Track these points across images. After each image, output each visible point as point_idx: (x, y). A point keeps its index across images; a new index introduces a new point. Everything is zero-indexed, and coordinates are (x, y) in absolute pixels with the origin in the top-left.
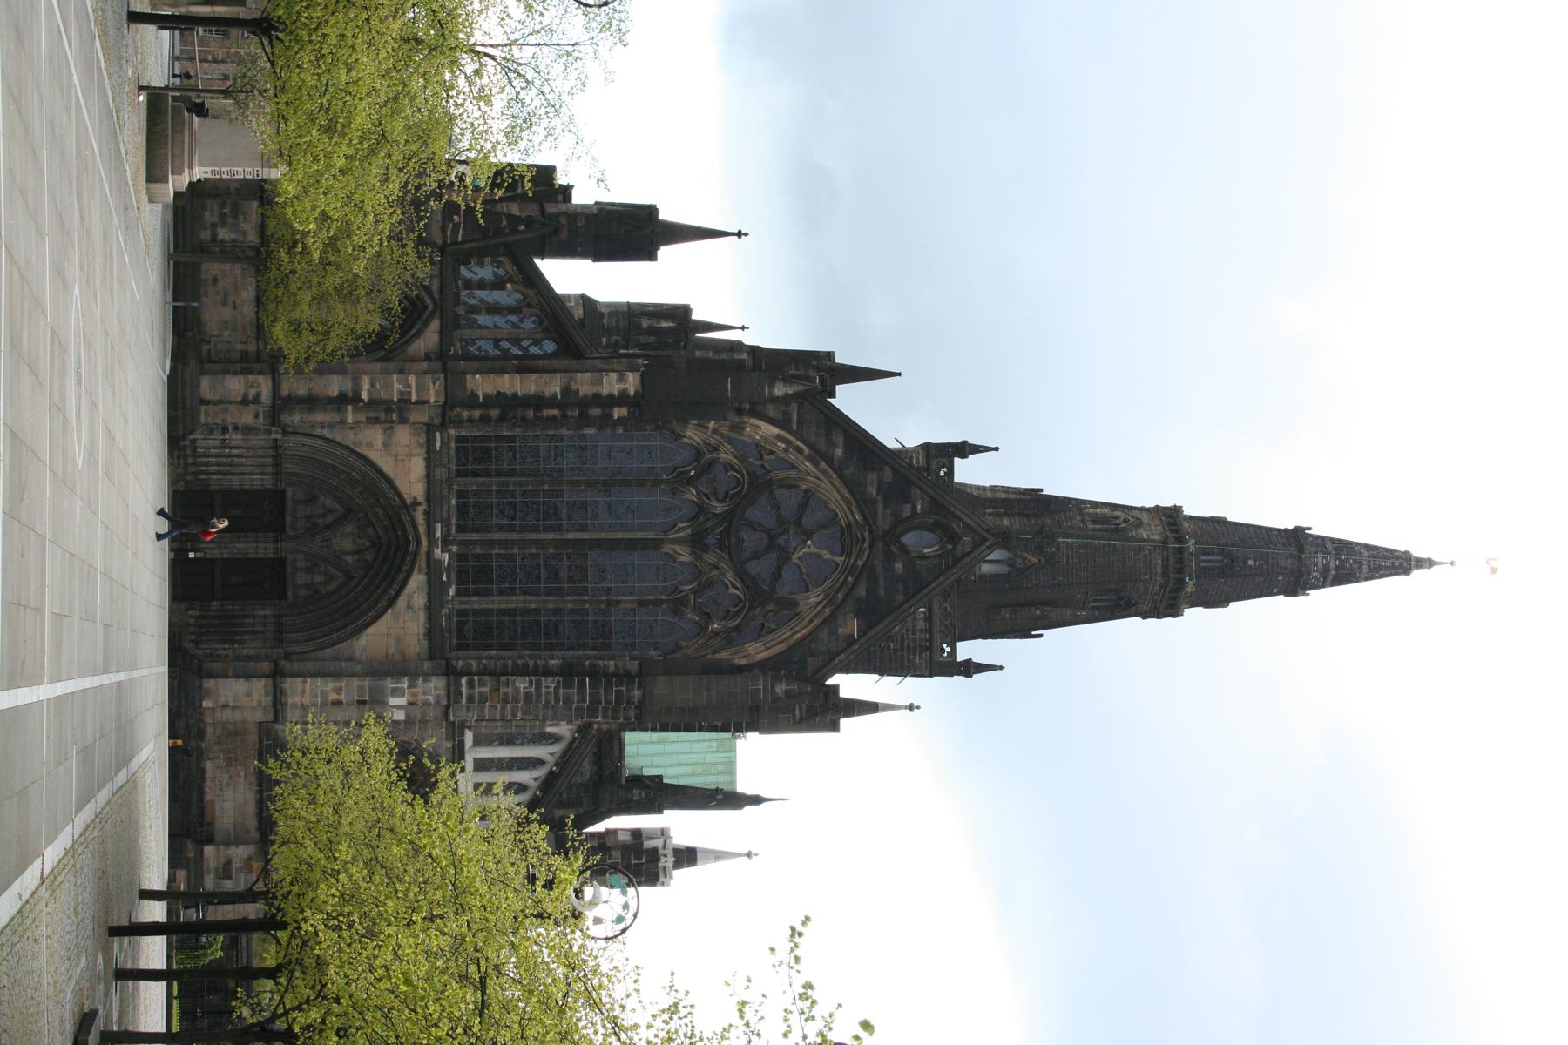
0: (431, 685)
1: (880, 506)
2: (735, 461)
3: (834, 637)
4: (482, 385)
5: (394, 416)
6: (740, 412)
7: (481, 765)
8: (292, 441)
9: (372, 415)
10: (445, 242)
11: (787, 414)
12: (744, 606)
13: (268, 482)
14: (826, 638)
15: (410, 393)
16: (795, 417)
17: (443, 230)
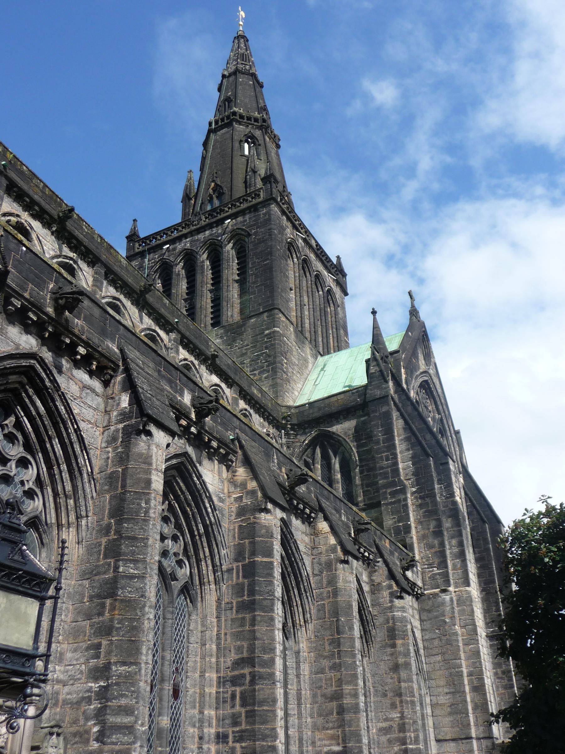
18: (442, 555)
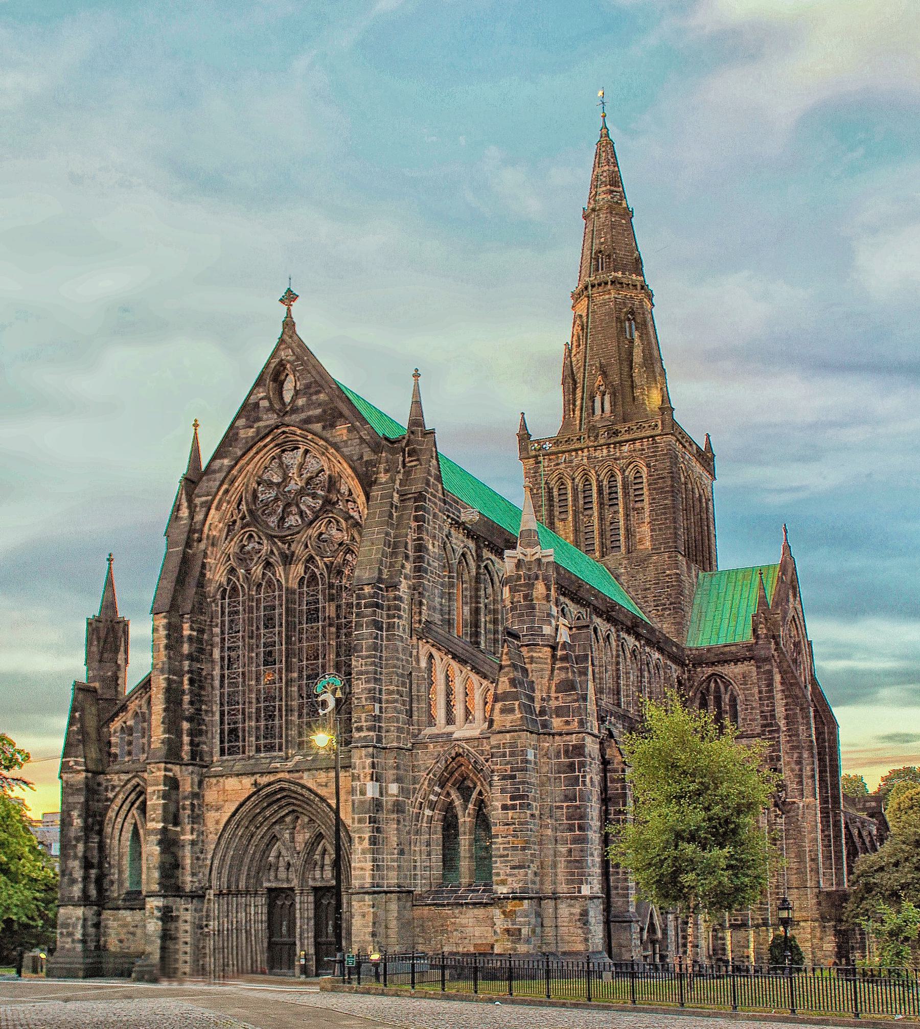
0: (358, 762)
1: (261, 424)
2: (235, 539)
3: (349, 442)
4: (158, 734)
5: (188, 802)
6: (200, 540)
7: (450, 720)
8: (214, 882)
9: (186, 820)
10: (87, 771)
11: (202, 503)
12: (332, 517)
13: (262, 900)
14: (349, 449)
15: (159, 791)
16: (204, 499)
17: (79, 772)
18: (800, 776)
